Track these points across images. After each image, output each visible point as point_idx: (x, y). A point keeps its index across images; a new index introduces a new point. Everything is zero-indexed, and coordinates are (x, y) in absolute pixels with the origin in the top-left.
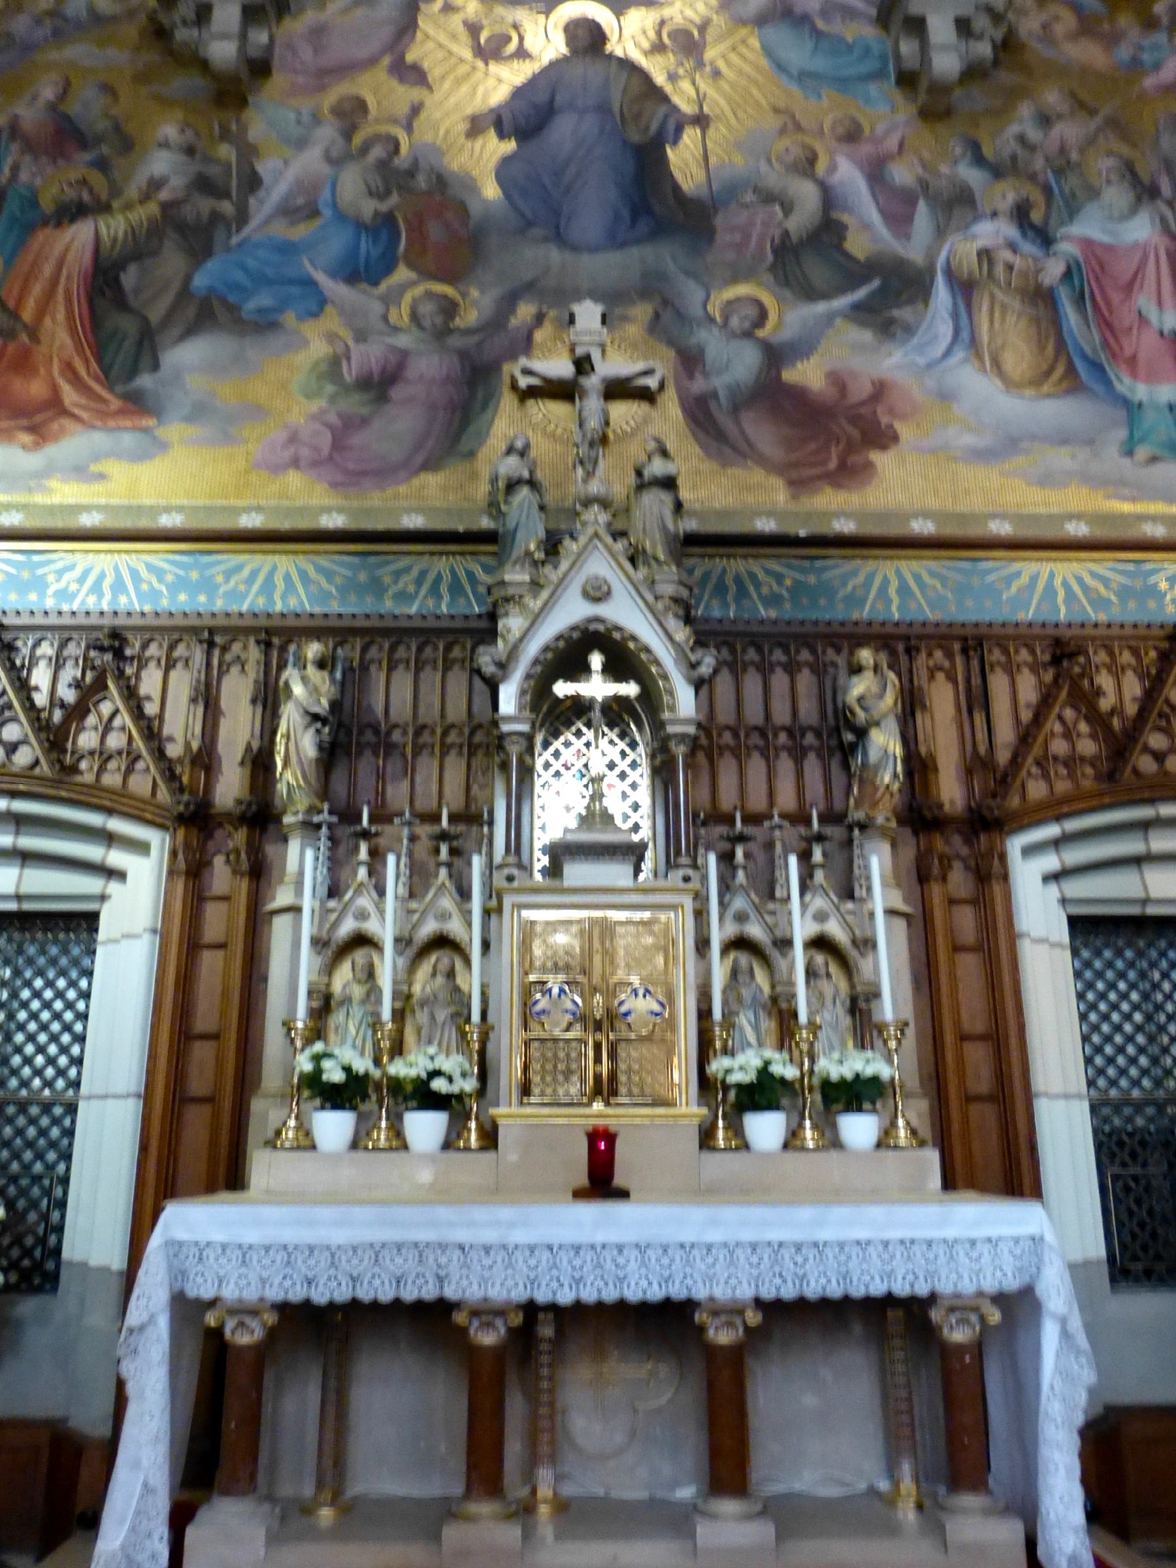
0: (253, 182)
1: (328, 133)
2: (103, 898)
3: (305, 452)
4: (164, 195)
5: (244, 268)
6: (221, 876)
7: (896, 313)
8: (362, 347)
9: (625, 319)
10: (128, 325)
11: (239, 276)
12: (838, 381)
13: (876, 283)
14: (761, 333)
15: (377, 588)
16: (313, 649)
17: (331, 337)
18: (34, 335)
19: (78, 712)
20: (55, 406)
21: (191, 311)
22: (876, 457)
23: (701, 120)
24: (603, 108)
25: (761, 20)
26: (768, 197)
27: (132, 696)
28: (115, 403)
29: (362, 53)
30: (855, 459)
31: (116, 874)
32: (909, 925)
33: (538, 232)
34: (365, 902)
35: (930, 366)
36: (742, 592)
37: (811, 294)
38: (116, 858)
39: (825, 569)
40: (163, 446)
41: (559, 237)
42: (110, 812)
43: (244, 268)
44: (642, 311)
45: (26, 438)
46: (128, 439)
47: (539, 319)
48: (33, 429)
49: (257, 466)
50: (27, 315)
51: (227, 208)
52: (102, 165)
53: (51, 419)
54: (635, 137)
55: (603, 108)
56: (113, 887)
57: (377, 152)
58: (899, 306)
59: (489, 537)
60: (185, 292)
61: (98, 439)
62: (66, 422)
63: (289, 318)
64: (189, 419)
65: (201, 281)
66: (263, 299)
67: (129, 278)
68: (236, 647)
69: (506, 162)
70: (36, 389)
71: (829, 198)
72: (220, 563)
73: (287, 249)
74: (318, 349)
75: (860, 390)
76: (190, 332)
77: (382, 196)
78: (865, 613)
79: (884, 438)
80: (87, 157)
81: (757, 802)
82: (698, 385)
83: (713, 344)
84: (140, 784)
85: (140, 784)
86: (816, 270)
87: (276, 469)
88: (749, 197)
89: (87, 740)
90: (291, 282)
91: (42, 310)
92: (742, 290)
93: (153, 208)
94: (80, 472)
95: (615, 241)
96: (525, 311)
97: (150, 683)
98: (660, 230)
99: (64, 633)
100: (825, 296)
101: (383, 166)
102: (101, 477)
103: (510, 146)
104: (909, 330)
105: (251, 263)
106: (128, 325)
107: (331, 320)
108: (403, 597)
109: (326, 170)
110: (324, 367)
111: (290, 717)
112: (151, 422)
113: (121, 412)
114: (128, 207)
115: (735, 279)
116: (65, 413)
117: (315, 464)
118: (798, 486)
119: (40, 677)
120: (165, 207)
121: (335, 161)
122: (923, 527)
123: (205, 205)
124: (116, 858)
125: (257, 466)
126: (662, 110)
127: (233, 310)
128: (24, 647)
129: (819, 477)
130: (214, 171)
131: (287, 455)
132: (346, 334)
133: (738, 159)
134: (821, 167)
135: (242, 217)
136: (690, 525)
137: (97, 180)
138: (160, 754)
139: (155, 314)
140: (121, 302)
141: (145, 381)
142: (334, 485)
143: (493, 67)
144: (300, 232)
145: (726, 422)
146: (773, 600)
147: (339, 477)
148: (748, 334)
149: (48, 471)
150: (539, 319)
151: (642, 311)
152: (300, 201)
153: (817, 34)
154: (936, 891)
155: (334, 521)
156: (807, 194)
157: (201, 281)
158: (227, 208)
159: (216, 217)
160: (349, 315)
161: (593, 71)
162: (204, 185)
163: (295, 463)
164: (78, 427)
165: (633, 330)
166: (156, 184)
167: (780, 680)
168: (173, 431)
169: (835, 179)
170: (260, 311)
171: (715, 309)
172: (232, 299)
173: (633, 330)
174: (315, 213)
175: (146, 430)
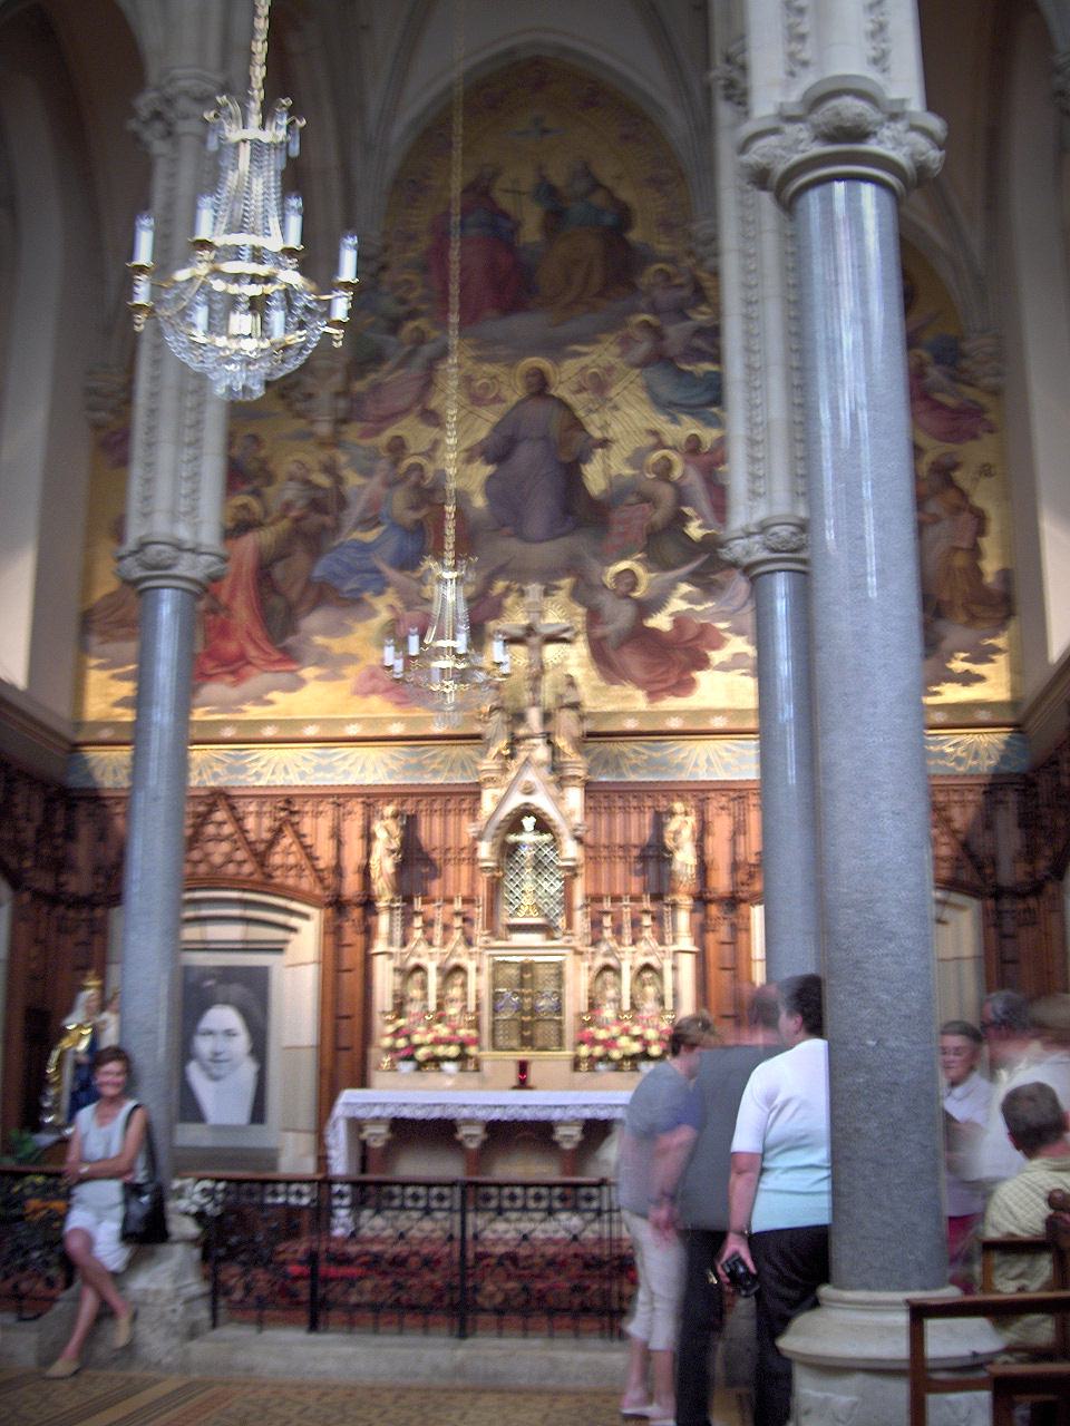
0: (343, 503)
1: (383, 465)
2: (286, 942)
3: (382, 685)
4: (294, 514)
5: (337, 560)
6: (351, 935)
7: (713, 577)
8: (410, 613)
9: (558, 588)
10: (277, 602)
11: (338, 569)
12: (679, 620)
13: (706, 557)
14: (636, 594)
15: (420, 767)
16: (389, 810)
17: (392, 607)
18: (227, 608)
19: (272, 843)
20: (242, 658)
21: (311, 595)
22: (698, 675)
23: (604, 443)
24: (545, 438)
25: (644, 364)
26: (648, 499)
27: (299, 836)
28: (277, 656)
29: (402, 403)
30: (685, 677)
31: (293, 930)
32: (697, 957)
33: (508, 530)
34: (423, 948)
35: (735, 611)
36: (618, 766)
37: (666, 566)
38: (294, 921)
39: (662, 749)
40: (301, 683)
41: (520, 535)
42: (292, 899)
43: (337, 560)
44: (566, 582)
45: (230, 679)
46: (284, 678)
47: (508, 590)
48: (232, 673)
49: (356, 692)
50: (224, 597)
51: (328, 520)
52: (257, 493)
53: (244, 665)
54: (568, 459)
55: (545, 438)
56: (292, 936)
57: (413, 478)
58: (714, 573)
59: (478, 736)
60: (309, 583)
61: (267, 678)
62: (248, 668)
63: (367, 595)
64: (316, 664)
65: (318, 572)
66: (351, 585)
67: (278, 572)
68: (349, 806)
69: (491, 478)
70: (232, 647)
71: (682, 497)
72: (335, 754)
73: (364, 548)
74: (384, 616)
75: (691, 633)
76: (315, 606)
77: (415, 507)
78: (684, 777)
79: (702, 663)
80: (248, 488)
81: (618, 890)
82: (599, 631)
83: (607, 603)
84: (307, 883)
85: (307, 883)
86: (670, 550)
87: (366, 694)
88: (632, 499)
89: (276, 859)
90: (366, 571)
91: (232, 596)
92: (623, 565)
93: (285, 524)
94: (260, 700)
95: (552, 535)
96: (500, 585)
97: (307, 825)
98: (579, 526)
99: (262, 798)
100: (674, 567)
101: (417, 486)
102: (270, 703)
103: (489, 469)
104: (722, 587)
105: (346, 559)
106: (277, 602)
107: (390, 597)
108: (435, 772)
109: (383, 491)
110: (388, 629)
111: (379, 848)
112: (294, 667)
113: (279, 661)
114: (272, 523)
115: (623, 557)
116: (249, 663)
117: (387, 690)
118: (653, 695)
119: (250, 823)
120: (297, 520)
121: (390, 484)
122: (718, 723)
123: (316, 519)
124: (294, 921)
125: (356, 692)
126: (580, 436)
127: (336, 590)
128: (240, 804)
129: (663, 690)
130: (320, 494)
131: (370, 685)
132: (399, 605)
133: (628, 471)
134: (677, 474)
135: (337, 529)
136: (588, 726)
137: (255, 505)
138: (315, 870)
139: (294, 594)
140: (274, 589)
141: (290, 641)
142: (398, 704)
143: (484, 412)
144: (370, 536)
145: (613, 655)
146: (635, 768)
147: (398, 700)
148: (626, 596)
149: (242, 701)
150: (508, 590)
151: (566, 582)
152: (370, 515)
153: (681, 373)
154: (711, 938)
155: (396, 729)
156: (666, 492)
157: (318, 572)
158: (328, 520)
159: (324, 527)
160: (402, 593)
161: (538, 409)
162: (316, 505)
163: (374, 691)
164: (255, 671)
165: (562, 596)
166: (288, 506)
167: (634, 818)
168: (308, 672)
169: (685, 482)
170: (352, 591)
171: (608, 579)
172: (337, 583)
173: (562, 596)
174: (379, 524)
175: (292, 671)
